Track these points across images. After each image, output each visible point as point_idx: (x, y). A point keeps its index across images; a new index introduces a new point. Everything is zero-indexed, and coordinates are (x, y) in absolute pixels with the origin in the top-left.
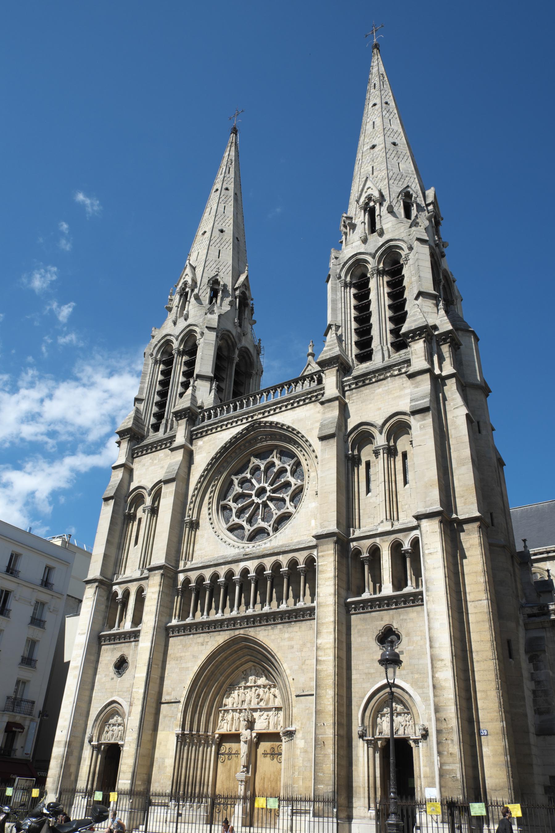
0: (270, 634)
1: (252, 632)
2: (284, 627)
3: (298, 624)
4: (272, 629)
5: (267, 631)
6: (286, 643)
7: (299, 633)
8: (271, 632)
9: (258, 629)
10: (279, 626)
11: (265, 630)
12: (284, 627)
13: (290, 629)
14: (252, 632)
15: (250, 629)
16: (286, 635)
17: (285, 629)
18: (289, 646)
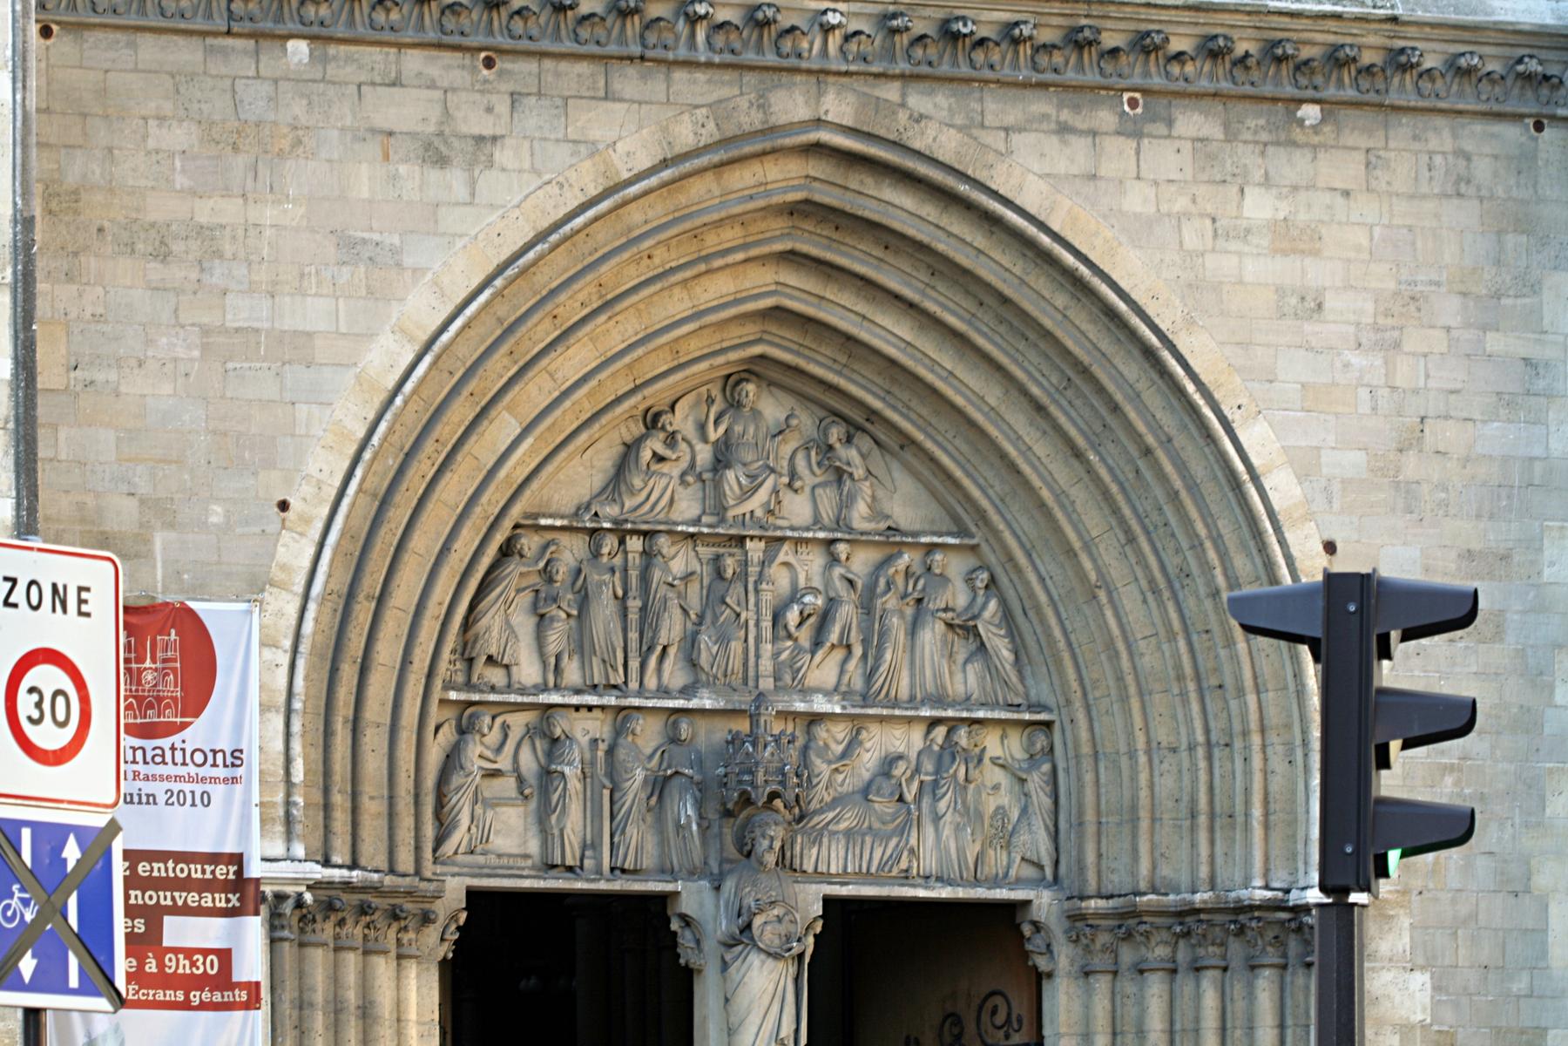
0: (1108, 168)
1: (935, 124)
2: (1231, 136)
3: (1357, 134)
4: (1133, 131)
5: (1080, 144)
6: (1260, 268)
7: (1366, 209)
8: (1118, 155)
9: (997, 108)
10: (1192, 123)
11: (1064, 130)
12: (1231, 136)
13: (1292, 166)
14: (935, 124)
15: (918, 101)
16: (1259, 207)
17: (1247, 156)
18: (1280, 291)
